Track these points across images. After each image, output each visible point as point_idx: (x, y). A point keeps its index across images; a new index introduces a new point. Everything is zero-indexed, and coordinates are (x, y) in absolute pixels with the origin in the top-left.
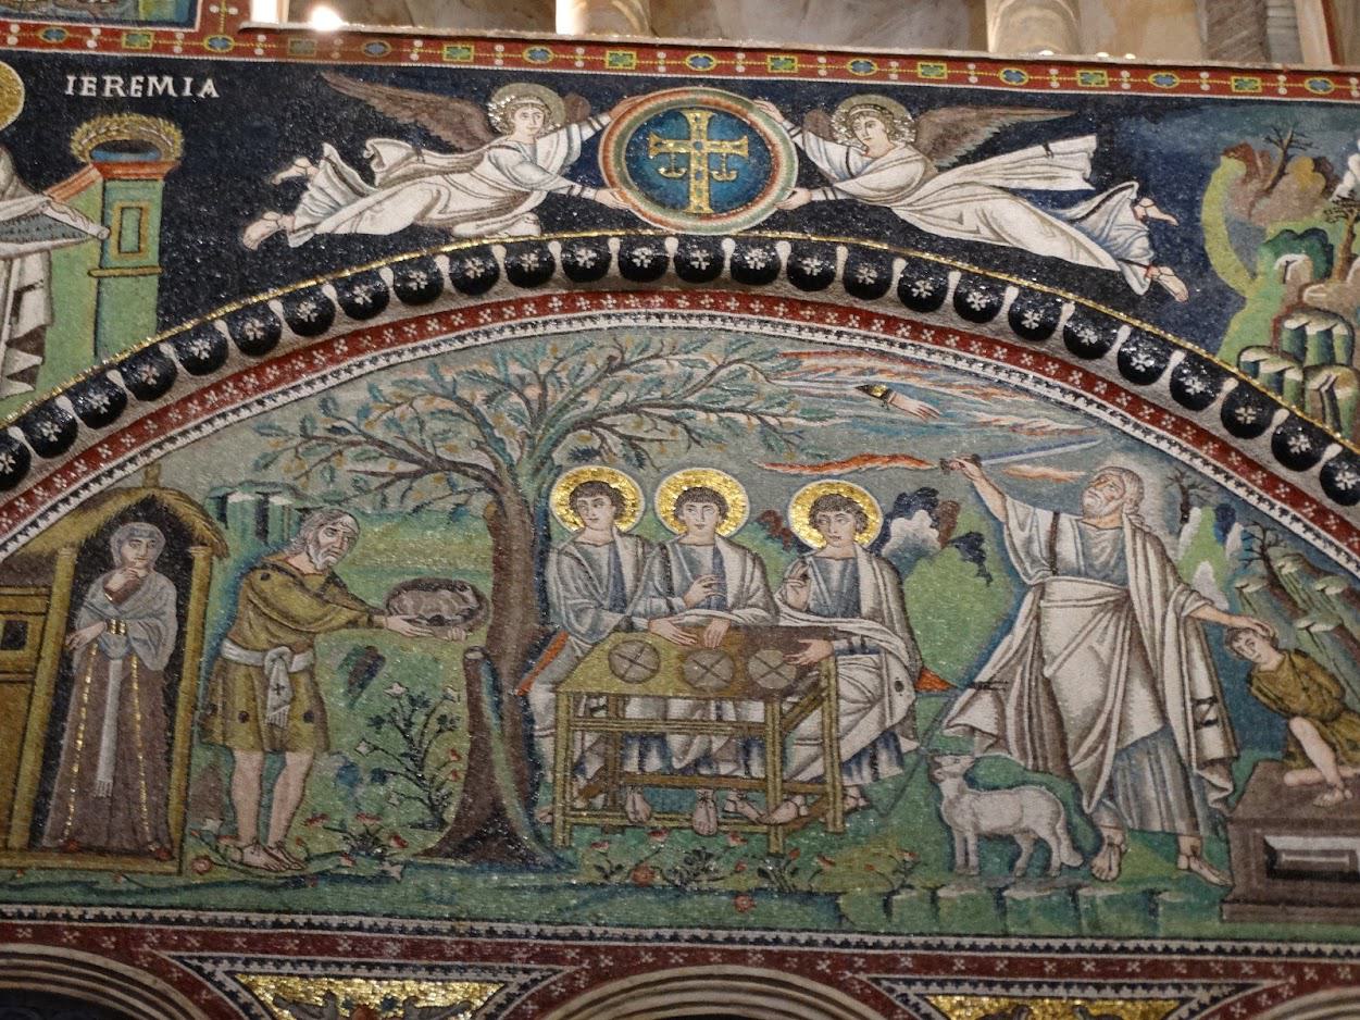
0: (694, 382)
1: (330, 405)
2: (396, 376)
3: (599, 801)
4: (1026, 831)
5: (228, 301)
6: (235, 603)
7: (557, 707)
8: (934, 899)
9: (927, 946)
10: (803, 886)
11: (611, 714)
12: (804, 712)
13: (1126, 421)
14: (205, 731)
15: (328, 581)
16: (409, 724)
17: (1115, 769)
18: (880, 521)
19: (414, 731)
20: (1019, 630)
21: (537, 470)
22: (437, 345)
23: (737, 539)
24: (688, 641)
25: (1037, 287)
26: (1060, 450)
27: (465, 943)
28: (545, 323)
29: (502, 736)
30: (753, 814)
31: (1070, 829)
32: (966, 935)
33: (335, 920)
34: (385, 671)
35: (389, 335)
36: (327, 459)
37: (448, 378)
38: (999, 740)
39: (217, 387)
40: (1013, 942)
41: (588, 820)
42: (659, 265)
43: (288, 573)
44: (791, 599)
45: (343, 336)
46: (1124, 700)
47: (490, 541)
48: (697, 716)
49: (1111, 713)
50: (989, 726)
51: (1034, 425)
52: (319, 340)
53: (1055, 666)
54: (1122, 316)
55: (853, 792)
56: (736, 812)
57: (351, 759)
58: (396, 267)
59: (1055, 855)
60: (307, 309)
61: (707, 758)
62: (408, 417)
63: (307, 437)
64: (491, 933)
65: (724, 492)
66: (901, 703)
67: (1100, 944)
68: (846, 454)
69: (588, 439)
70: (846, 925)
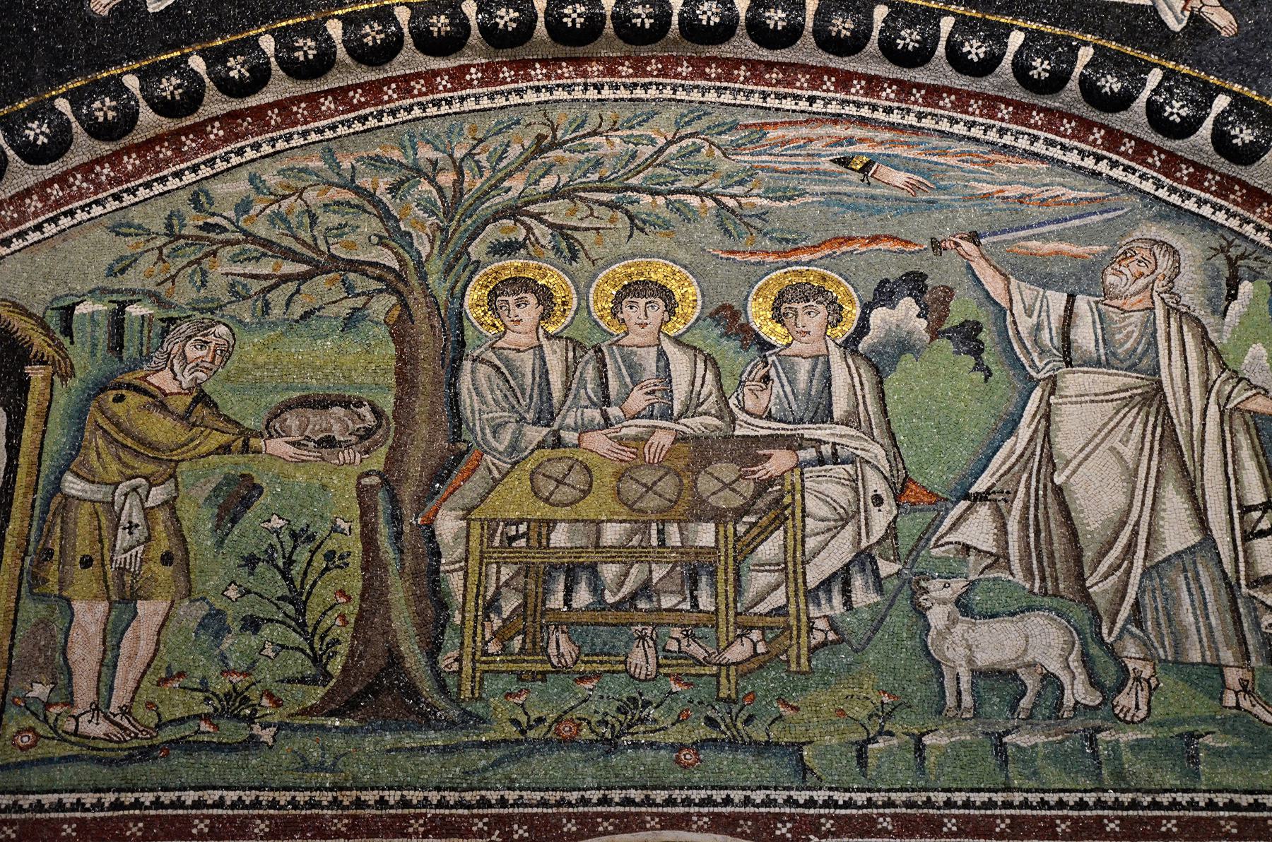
0: (638, 161)
1: (203, 199)
2: (285, 163)
3: (517, 643)
4: (1028, 665)
5: (73, 76)
6: (81, 430)
7: (468, 537)
8: (919, 748)
9: (910, 804)
10: (762, 738)
11: (534, 543)
12: (764, 534)
13: (1159, 185)
14: (37, 579)
15: (196, 401)
16: (290, 562)
17: (1142, 590)
18: (857, 312)
19: (296, 571)
20: (1024, 432)
21: (449, 269)
22: (333, 128)
23: (685, 339)
24: (627, 456)
25: (1048, 29)
26: (1077, 222)
27: (347, 817)
28: (462, 99)
29: (401, 574)
30: (700, 654)
31: (1086, 660)
32: (960, 790)
33: (190, 797)
34: (265, 499)
35: (274, 117)
36: (198, 261)
37: (346, 165)
38: (1000, 559)
39: (62, 179)
40: (1017, 798)
41: (503, 667)
42: (593, 27)
43: (145, 392)
44: (749, 404)
45: (217, 118)
46: (1152, 509)
47: (392, 349)
48: (635, 542)
49: (1137, 523)
50: (986, 542)
51: (1046, 195)
52: (188, 122)
53: (1067, 472)
54: (1154, 58)
55: (822, 624)
56: (680, 651)
57: (217, 606)
58: (279, 35)
59: (1067, 692)
60: (169, 86)
61: (645, 590)
62: (298, 210)
63: (173, 236)
64: (382, 803)
65: (672, 285)
66: (880, 520)
67: (1126, 798)
68: (818, 237)
69: (512, 230)
70: (811, 780)
